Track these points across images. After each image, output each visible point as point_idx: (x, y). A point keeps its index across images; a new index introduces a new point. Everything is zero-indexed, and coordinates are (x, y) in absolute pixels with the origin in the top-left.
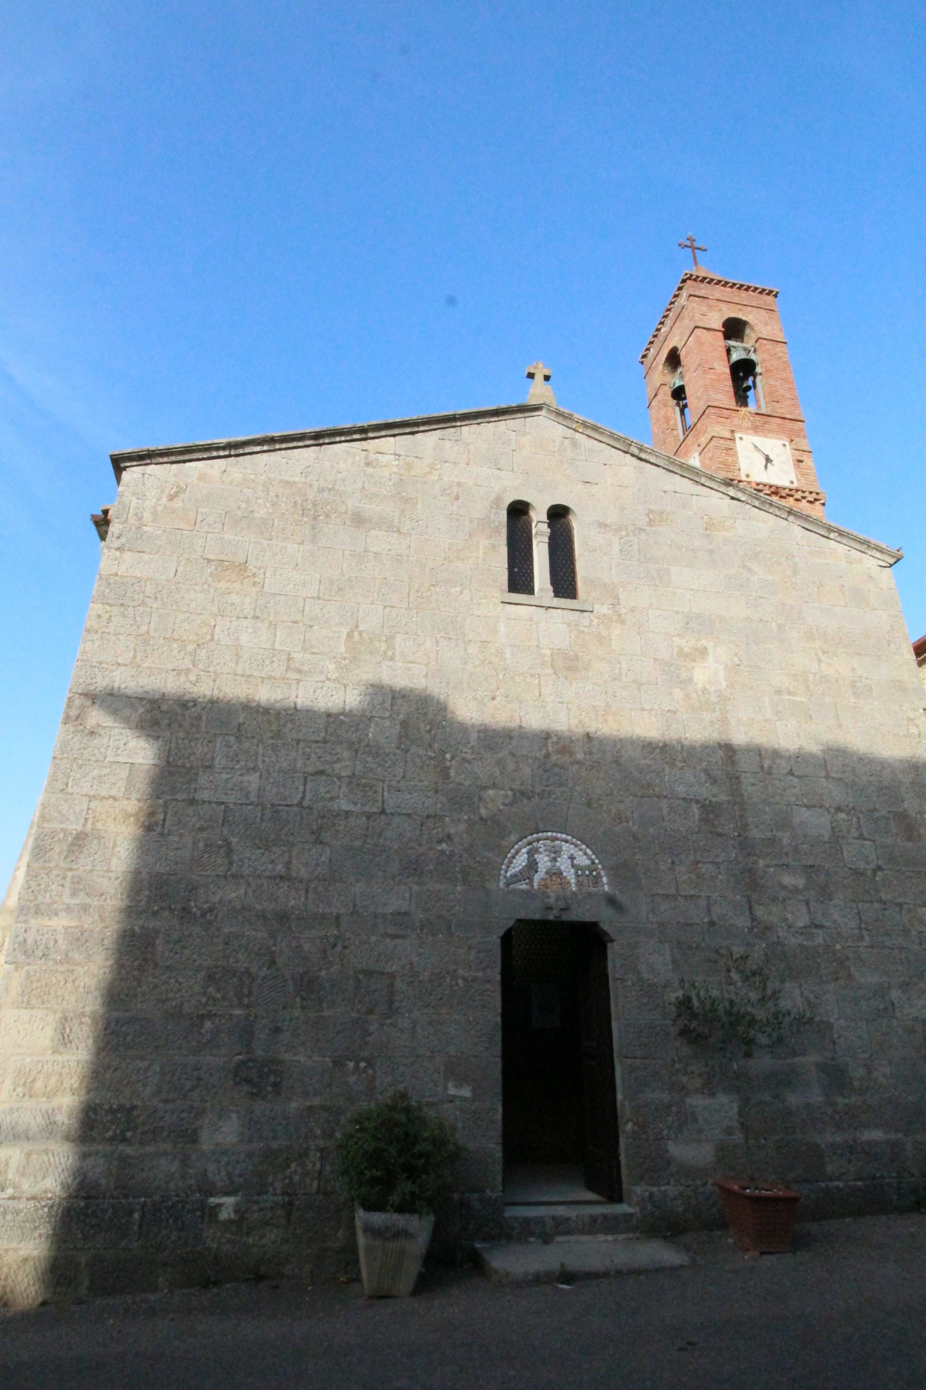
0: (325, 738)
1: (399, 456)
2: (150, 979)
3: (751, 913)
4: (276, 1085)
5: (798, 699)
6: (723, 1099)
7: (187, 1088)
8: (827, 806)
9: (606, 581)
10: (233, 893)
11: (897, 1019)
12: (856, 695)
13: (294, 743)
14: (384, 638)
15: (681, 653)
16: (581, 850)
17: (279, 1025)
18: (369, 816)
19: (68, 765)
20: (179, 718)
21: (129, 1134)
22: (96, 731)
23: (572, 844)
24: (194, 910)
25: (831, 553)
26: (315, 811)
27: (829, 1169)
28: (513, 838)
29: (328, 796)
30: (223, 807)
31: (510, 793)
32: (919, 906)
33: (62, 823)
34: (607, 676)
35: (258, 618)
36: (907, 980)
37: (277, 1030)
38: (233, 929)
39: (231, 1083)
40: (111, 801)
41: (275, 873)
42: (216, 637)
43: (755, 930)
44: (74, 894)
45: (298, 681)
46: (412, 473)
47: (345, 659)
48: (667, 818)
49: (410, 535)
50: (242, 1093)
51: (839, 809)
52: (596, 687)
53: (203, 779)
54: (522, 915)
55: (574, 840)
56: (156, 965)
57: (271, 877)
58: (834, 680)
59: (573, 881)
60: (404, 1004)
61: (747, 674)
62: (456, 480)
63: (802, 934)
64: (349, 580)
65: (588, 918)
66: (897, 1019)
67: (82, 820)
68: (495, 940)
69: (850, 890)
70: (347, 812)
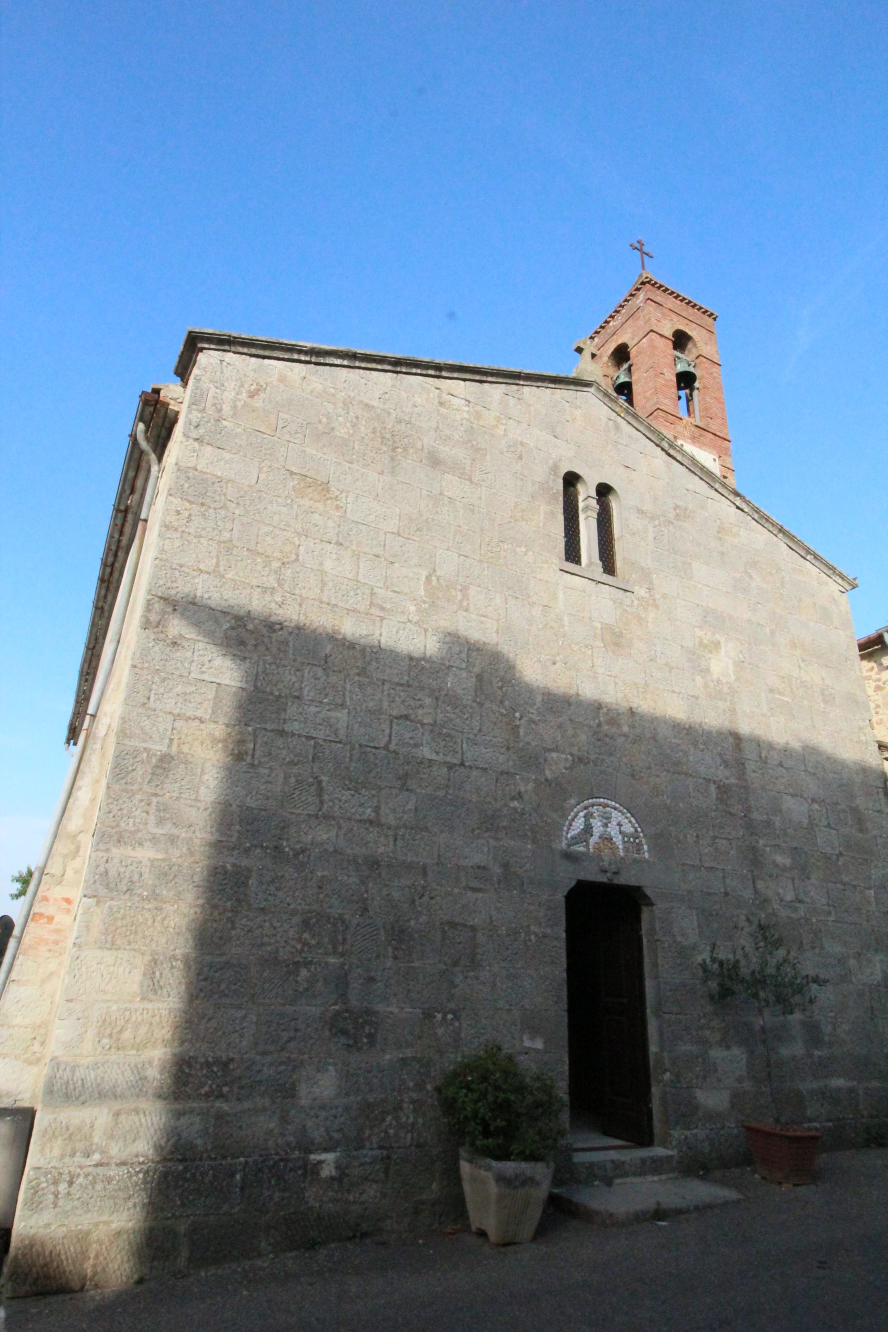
0: (408, 681)
1: (469, 402)
3: (754, 887)
4: (371, 1036)
6: (736, 1051)
7: (285, 1039)
9: (643, 565)
10: (323, 834)
12: (826, 702)
13: (380, 683)
14: (459, 587)
16: (627, 818)
17: (373, 974)
18: (451, 766)
19: (149, 677)
20: (266, 640)
21: (225, 1089)
22: (179, 642)
23: (620, 811)
24: (287, 849)
26: (401, 756)
27: (809, 1112)
28: (573, 801)
30: (312, 742)
33: (145, 741)
34: (645, 656)
35: (341, 544)
37: (372, 980)
38: (326, 873)
39: (327, 1033)
40: (197, 723)
41: (365, 817)
42: (300, 558)
44: (160, 822)
45: (382, 619)
47: (424, 602)
48: (692, 794)
49: (481, 486)
50: (340, 1045)
53: (292, 710)
55: (621, 808)
57: (361, 821)
59: (621, 847)
62: (520, 439)
63: (790, 907)
64: (427, 521)
65: (633, 882)
67: (167, 741)
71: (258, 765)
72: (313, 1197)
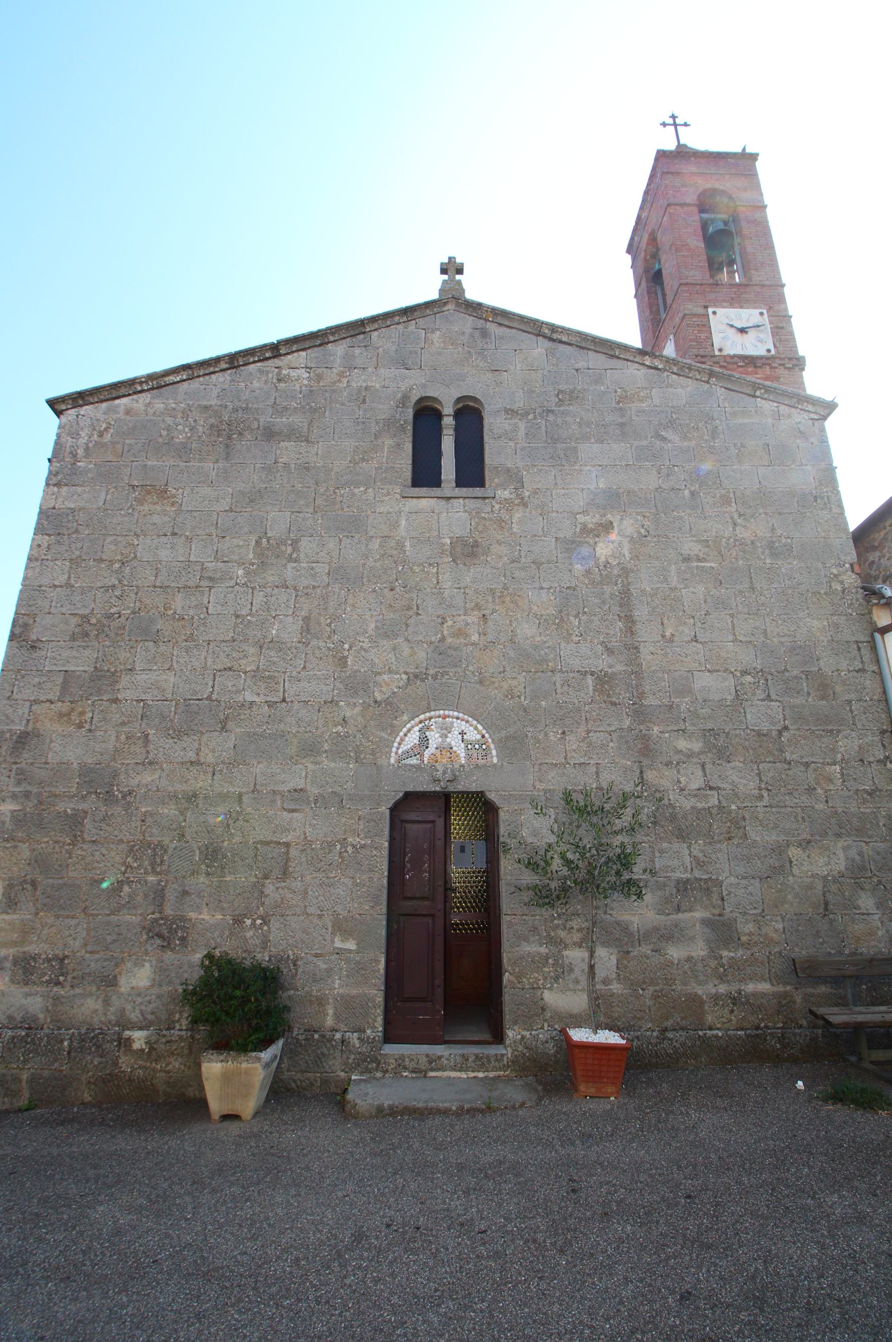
0: (233, 637)
1: (311, 368)
2: (79, 852)
4: (183, 939)
5: (708, 565)
7: (109, 941)
8: (733, 670)
9: (510, 466)
11: (794, 876)
12: (774, 555)
13: (205, 644)
14: (289, 542)
15: (585, 530)
16: (471, 725)
17: (187, 888)
18: (270, 704)
19: (13, 676)
20: (106, 629)
21: (62, 979)
22: (36, 645)
23: (463, 720)
24: (116, 793)
25: (756, 412)
26: (223, 704)
28: (405, 718)
29: (234, 689)
31: (404, 677)
32: (828, 764)
33: (8, 725)
34: (506, 558)
35: (176, 534)
36: (809, 837)
38: (150, 809)
39: (145, 937)
40: (48, 704)
42: (138, 554)
43: (645, 794)
44: (19, 783)
45: (210, 588)
46: (321, 384)
47: (253, 564)
48: (559, 691)
49: (318, 442)
50: (155, 946)
51: (745, 673)
52: (494, 571)
53: (125, 680)
54: (410, 788)
55: (466, 717)
56: (84, 841)
57: (182, 763)
58: (749, 542)
59: (463, 755)
60: (297, 869)
61: (653, 544)
62: (364, 385)
63: (696, 796)
65: (473, 788)
66: (794, 876)
67: (25, 722)
68: (384, 810)
69: (751, 752)
70: (252, 703)
71: (95, 730)
72: (125, 1063)
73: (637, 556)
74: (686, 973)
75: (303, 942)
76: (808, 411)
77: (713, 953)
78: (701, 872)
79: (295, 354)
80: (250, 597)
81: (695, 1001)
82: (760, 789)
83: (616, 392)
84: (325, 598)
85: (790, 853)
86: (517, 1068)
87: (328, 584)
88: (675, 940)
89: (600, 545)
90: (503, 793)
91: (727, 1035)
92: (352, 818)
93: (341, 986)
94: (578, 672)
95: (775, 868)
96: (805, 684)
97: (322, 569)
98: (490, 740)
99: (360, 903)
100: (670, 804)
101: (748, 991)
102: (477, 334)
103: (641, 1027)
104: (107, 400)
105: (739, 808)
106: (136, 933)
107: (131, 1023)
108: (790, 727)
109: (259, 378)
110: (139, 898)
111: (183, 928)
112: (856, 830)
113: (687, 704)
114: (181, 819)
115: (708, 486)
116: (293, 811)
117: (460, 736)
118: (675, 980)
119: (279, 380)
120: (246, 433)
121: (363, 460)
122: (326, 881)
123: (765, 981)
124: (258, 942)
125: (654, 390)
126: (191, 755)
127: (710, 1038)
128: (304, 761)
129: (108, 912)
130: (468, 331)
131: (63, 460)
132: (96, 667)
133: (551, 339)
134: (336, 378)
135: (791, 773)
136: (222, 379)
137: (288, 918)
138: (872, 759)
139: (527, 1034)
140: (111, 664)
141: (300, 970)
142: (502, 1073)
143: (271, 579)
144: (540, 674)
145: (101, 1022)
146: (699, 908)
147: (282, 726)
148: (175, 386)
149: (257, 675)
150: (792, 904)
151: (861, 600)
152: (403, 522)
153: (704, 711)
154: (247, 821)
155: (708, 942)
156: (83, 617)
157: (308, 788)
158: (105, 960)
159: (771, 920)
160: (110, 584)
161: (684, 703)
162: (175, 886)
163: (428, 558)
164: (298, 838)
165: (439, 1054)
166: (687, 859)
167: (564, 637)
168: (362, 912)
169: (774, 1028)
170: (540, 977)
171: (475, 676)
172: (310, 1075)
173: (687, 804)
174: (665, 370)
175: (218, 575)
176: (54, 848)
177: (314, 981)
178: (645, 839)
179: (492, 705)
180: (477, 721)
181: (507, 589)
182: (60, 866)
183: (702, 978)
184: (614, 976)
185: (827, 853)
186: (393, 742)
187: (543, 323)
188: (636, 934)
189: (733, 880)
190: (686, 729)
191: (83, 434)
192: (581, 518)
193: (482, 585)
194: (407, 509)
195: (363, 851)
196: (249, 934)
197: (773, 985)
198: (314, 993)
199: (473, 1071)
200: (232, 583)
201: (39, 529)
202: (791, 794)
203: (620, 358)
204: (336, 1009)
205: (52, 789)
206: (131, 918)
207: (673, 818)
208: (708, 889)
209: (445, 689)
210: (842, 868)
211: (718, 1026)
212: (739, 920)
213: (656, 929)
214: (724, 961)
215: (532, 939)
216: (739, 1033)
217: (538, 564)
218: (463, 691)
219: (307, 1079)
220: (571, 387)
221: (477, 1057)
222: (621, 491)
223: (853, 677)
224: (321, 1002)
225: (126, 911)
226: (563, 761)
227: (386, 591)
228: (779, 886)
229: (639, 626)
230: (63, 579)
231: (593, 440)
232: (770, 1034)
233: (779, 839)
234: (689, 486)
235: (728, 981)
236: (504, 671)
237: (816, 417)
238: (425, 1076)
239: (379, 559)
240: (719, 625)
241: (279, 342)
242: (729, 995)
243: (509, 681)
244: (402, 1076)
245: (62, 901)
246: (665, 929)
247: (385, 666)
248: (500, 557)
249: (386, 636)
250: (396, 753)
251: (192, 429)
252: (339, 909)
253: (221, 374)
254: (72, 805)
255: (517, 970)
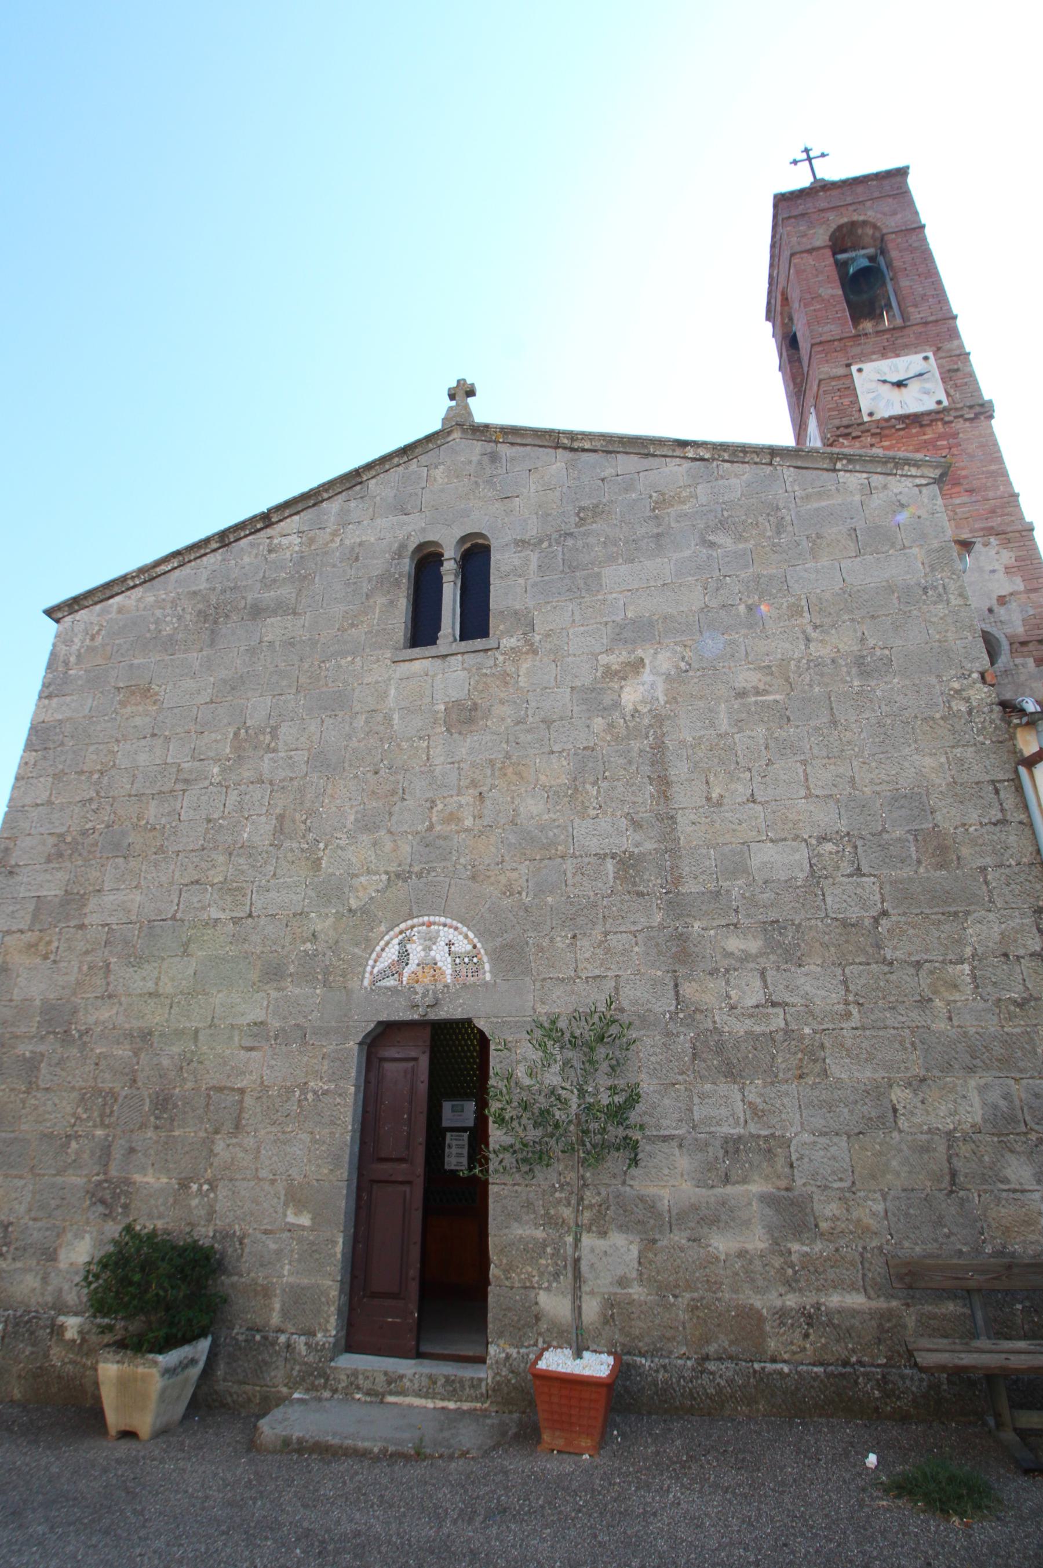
1: (303, 532)
2: (33, 1101)
3: (677, 993)
5: (771, 698)
6: (618, 1239)
7: (53, 1206)
8: (806, 836)
9: (517, 607)
10: (106, 1013)
11: (900, 1131)
14: (268, 730)
15: (609, 673)
17: (134, 1145)
18: (236, 921)
20: (80, 847)
23: (451, 927)
25: (838, 490)
27: (772, 1344)
28: (383, 928)
29: (199, 905)
30: (106, 929)
31: (384, 877)
32: (951, 962)
34: (509, 720)
35: (156, 735)
36: (922, 1073)
37: (132, 1150)
38: (104, 1050)
40: (18, 935)
41: (145, 991)
42: (117, 762)
43: (681, 1015)
45: (184, 791)
46: (313, 548)
48: (569, 882)
51: (823, 839)
52: (495, 737)
53: (92, 903)
54: (384, 1017)
55: (455, 923)
56: (38, 1089)
57: (140, 995)
58: (829, 662)
59: (449, 972)
60: (251, 1121)
61: (696, 680)
62: (358, 540)
63: (751, 1016)
64: (241, 677)
65: (458, 1014)
66: (900, 1131)
68: (352, 1045)
69: (833, 949)
70: (217, 920)
71: (60, 961)
72: (57, 1356)
73: (674, 698)
74: (737, 1274)
75: (252, 1214)
76: (911, 476)
77: (777, 1246)
78: (758, 1126)
79: (288, 520)
80: (223, 797)
81: (750, 1318)
82: (847, 1003)
83: (651, 497)
84: (301, 790)
85: (894, 1098)
86: (500, 1399)
87: (306, 774)
88: (722, 1225)
89: (627, 689)
90: (495, 1020)
91: (797, 1372)
92: (314, 1057)
93: (291, 1273)
94: (595, 855)
95: (871, 1119)
96: (913, 849)
97: (300, 757)
98: (482, 951)
99: (318, 1166)
100: (715, 1028)
101: (831, 1305)
102: (486, 458)
103: (671, 1352)
104: (101, 601)
105: (815, 1032)
106: (80, 1198)
107: (67, 1307)
108: (891, 911)
109: (250, 552)
110: (86, 1156)
111: (127, 1194)
112: (997, 1060)
113: (740, 888)
114: (135, 1061)
115: (770, 595)
116: (251, 1049)
117: (447, 948)
118: (722, 1284)
119: (270, 551)
120: (232, 615)
121: (353, 625)
122: (282, 1137)
123: (857, 1290)
124: (203, 1212)
125: (699, 487)
126: (150, 986)
127: (770, 1374)
128: (266, 987)
129: (54, 1172)
130: (475, 459)
131: (56, 670)
132: (66, 891)
133: (572, 450)
134: (328, 538)
135: (893, 977)
136: (212, 560)
137: (237, 1184)
138: (1021, 952)
139: (513, 1352)
140: (81, 885)
141: (247, 1250)
142: (479, 1405)
143: (246, 774)
144: (546, 861)
145: (38, 1303)
146: (756, 1178)
147: (246, 946)
148: (167, 575)
149: (226, 888)
150: (898, 1174)
151: (998, 722)
152: (393, 692)
153: (764, 896)
154: (201, 1063)
155: (770, 1229)
156: (61, 835)
157: (269, 1021)
158: (47, 1229)
159: (866, 1199)
160: (88, 797)
161: (736, 888)
162: (122, 1142)
163: (418, 731)
164: (254, 1082)
165: (401, 1372)
166: (739, 1107)
167: (578, 812)
168: (319, 1177)
169: (872, 1365)
170: (535, 1273)
171: (467, 870)
172: (248, 1388)
173: (739, 1027)
174: (714, 459)
175: (193, 777)
176: (9, 1097)
177: (262, 1265)
178: (680, 1078)
179: (487, 906)
180: (468, 927)
181: (509, 758)
182: (13, 1117)
183: (760, 1283)
184: (634, 1274)
185: (952, 1097)
186: (368, 959)
187: (559, 433)
188: (666, 1215)
189: (806, 1137)
190: (738, 922)
191: (76, 640)
192: (604, 659)
193: (480, 757)
194: (397, 675)
195: (326, 1099)
196: (194, 1202)
197: (869, 1298)
198: (260, 1281)
199: (442, 1399)
200: (206, 783)
201: (29, 746)
202: (894, 1008)
203: (656, 456)
204: (283, 1304)
205: (15, 1029)
206: (76, 1180)
207: (720, 1049)
208: (769, 1151)
209: (432, 889)
210: (978, 1119)
211: (786, 1356)
212: (816, 1197)
213: (695, 1208)
214: (794, 1258)
215: (525, 1218)
216: (815, 1369)
217: (548, 723)
218: (452, 890)
219: (245, 1393)
220: (595, 502)
221: (448, 1381)
222: (656, 617)
223: (988, 833)
224: (266, 1292)
225: (71, 1171)
226: (573, 974)
227: (369, 775)
228: (878, 1147)
229: (676, 788)
230: (44, 796)
231: (620, 561)
232: (865, 1374)
233: (876, 1076)
234: (745, 598)
235: (800, 1290)
236: (503, 861)
237: (924, 481)
238: (382, 1402)
239: (364, 738)
240: (785, 777)
241: (269, 510)
242: (802, 1311)
243: (508, 873)
244: (353, 1399)
245: (12, 1158)
246: (708, 1208)
247: (363, 866)
248: (503, 719)
249: (367, 829)
250: (371, 973)
251: (180, 618)
252: (294, 1172)
253: (212, 555)
254: (30, 1047)
255: (505, 1261)
